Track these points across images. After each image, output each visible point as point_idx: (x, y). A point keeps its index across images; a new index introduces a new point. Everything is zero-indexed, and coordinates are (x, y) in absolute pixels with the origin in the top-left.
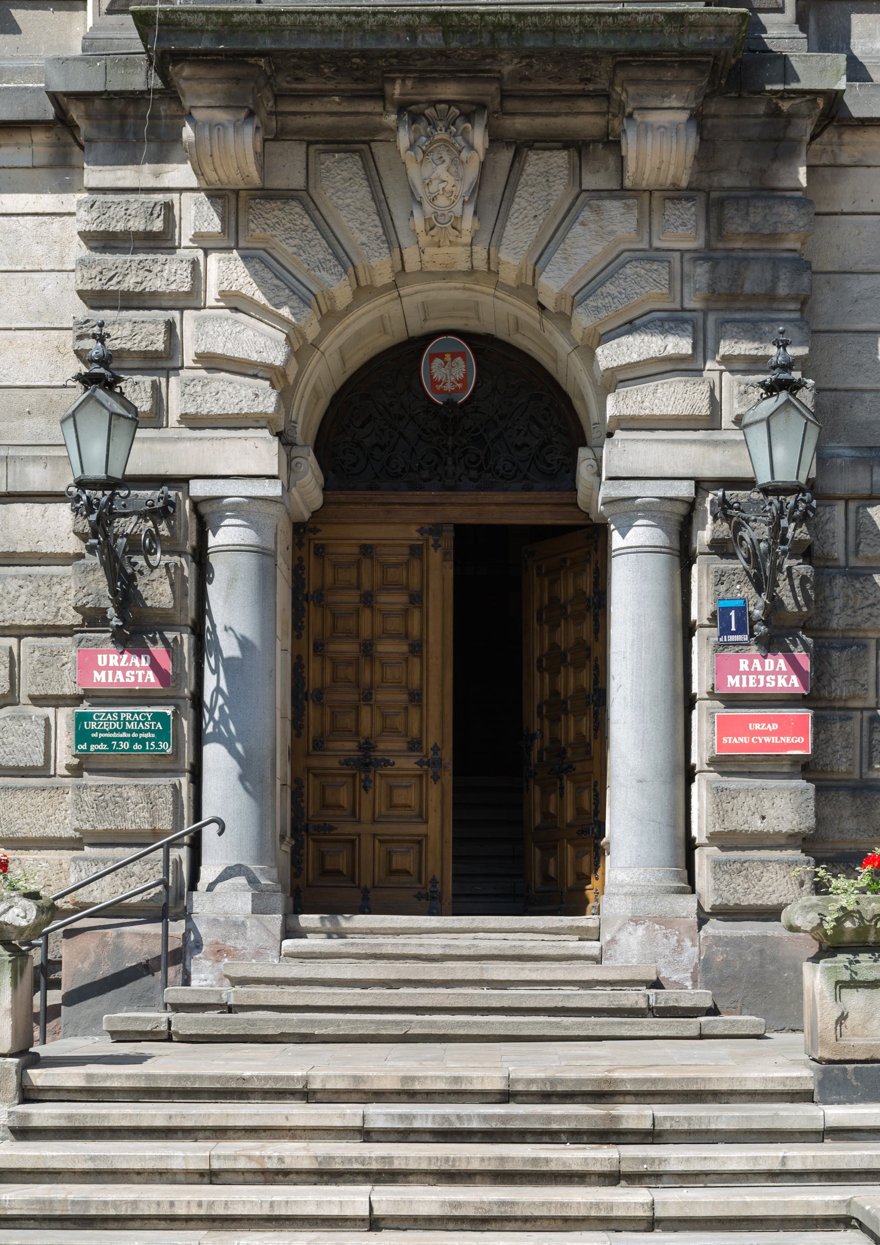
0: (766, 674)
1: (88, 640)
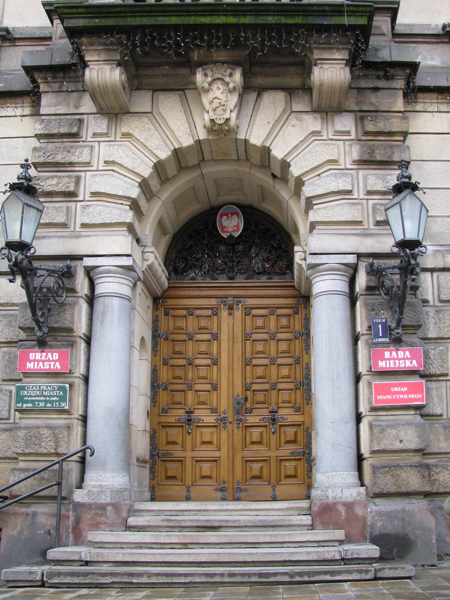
0: (399, 359)
1: (25, 345)
